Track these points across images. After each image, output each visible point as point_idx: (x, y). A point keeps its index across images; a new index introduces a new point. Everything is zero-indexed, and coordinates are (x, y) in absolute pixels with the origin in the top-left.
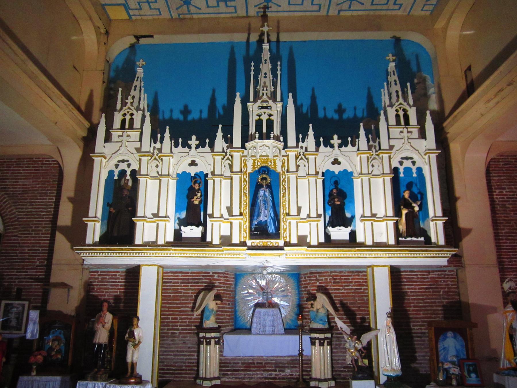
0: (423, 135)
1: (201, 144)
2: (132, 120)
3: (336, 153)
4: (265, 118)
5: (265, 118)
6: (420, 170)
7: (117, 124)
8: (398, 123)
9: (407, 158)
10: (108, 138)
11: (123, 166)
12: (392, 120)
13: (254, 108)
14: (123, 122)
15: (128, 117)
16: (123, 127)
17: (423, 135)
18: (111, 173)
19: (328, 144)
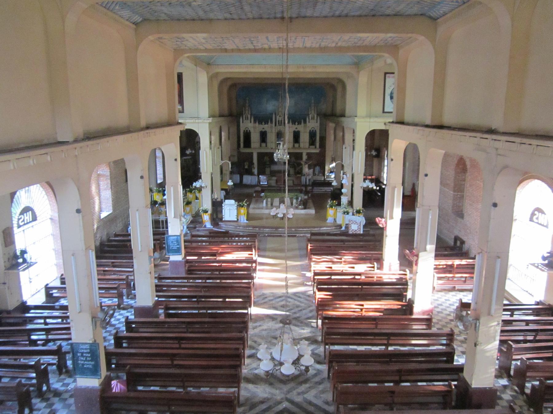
0: (317, 122)
1: (265, 124)
2: (248, 117)
3: (296, 126)
4: (280, 119)
5: (280, 119)
6: (315, 131)
7: (244, 119)
8: (312, 119)
9: (313, 128)
10: (243, 122)
11: (247, 129)
12: (310, 118)
13: (278, 117)
14: (246, 117)
15: (247, 116)
16: (246, 119)
17: (317, 122)
18: (244, 131)
19: (295, 124)
